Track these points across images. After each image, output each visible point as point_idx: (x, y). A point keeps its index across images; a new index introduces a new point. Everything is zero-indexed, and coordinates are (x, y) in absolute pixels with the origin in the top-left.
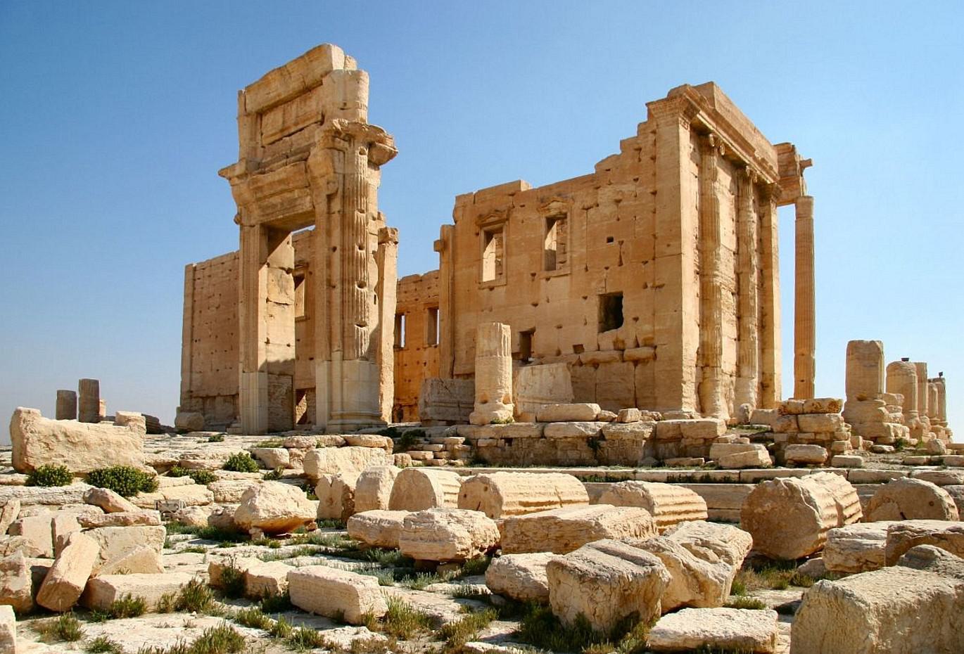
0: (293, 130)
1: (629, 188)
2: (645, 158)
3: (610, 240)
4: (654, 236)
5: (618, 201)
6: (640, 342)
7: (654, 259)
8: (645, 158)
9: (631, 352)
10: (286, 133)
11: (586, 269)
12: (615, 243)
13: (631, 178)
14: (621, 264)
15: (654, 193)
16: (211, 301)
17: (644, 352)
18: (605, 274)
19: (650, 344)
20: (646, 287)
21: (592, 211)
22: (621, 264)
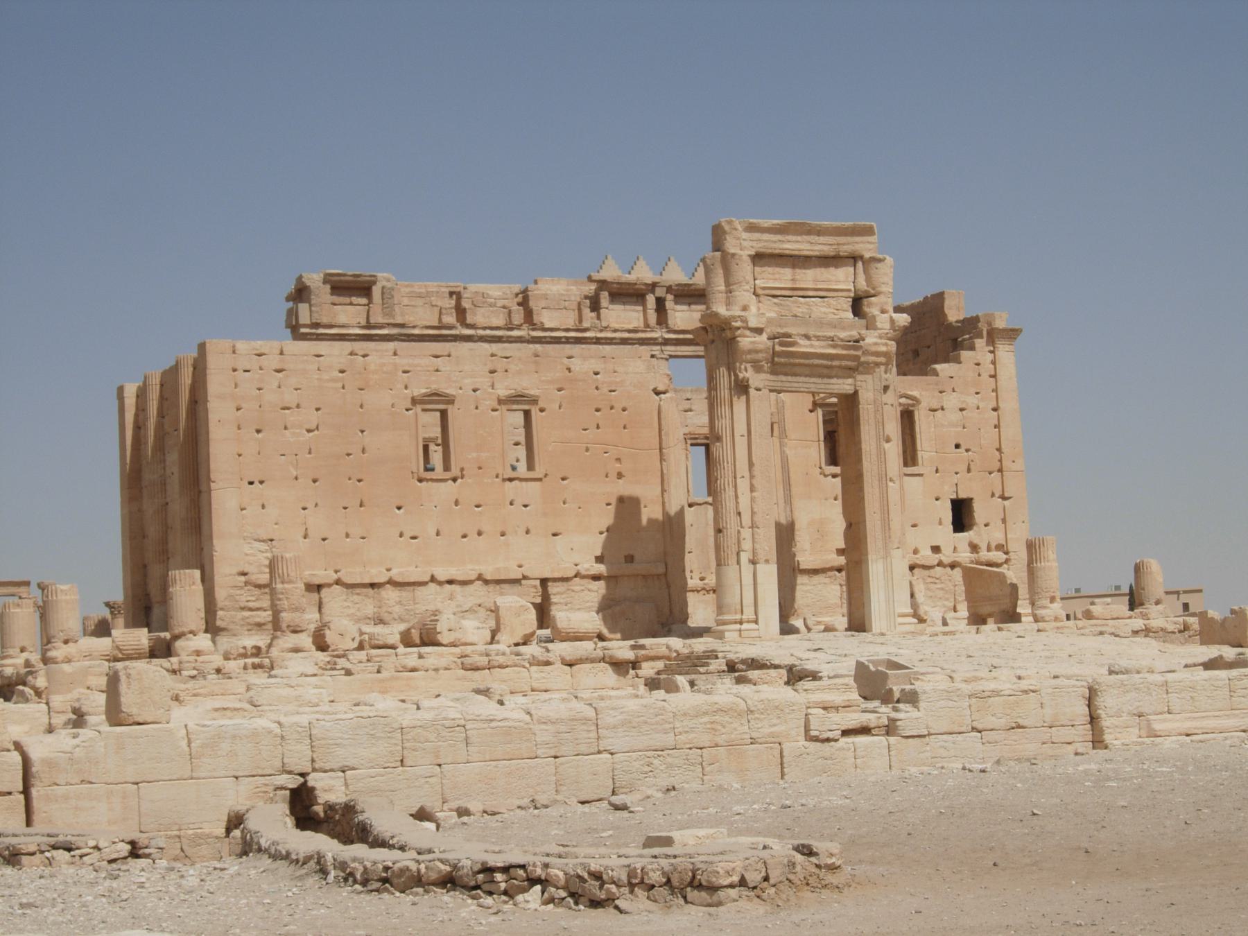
0: (811, 293)
1: (972, 400)
2: (985, 376)
3: (957, 446)
4: (999, 450)
5: (962, 410)
6: (993, 545)
7: (1000, 470)
8: (985, 376)
9: (984, 555)
10: (801, 293)
11: (937, 471)
12: (962, 450)
13: (973, 390)
14: (969, 470)
15: (995, 410)
16: (291, 417)
17: (998, 556)
18: (955, 479)
19: (999, 547)
20: (993, 495)
21: (939, 413)
22: (969, 470)
